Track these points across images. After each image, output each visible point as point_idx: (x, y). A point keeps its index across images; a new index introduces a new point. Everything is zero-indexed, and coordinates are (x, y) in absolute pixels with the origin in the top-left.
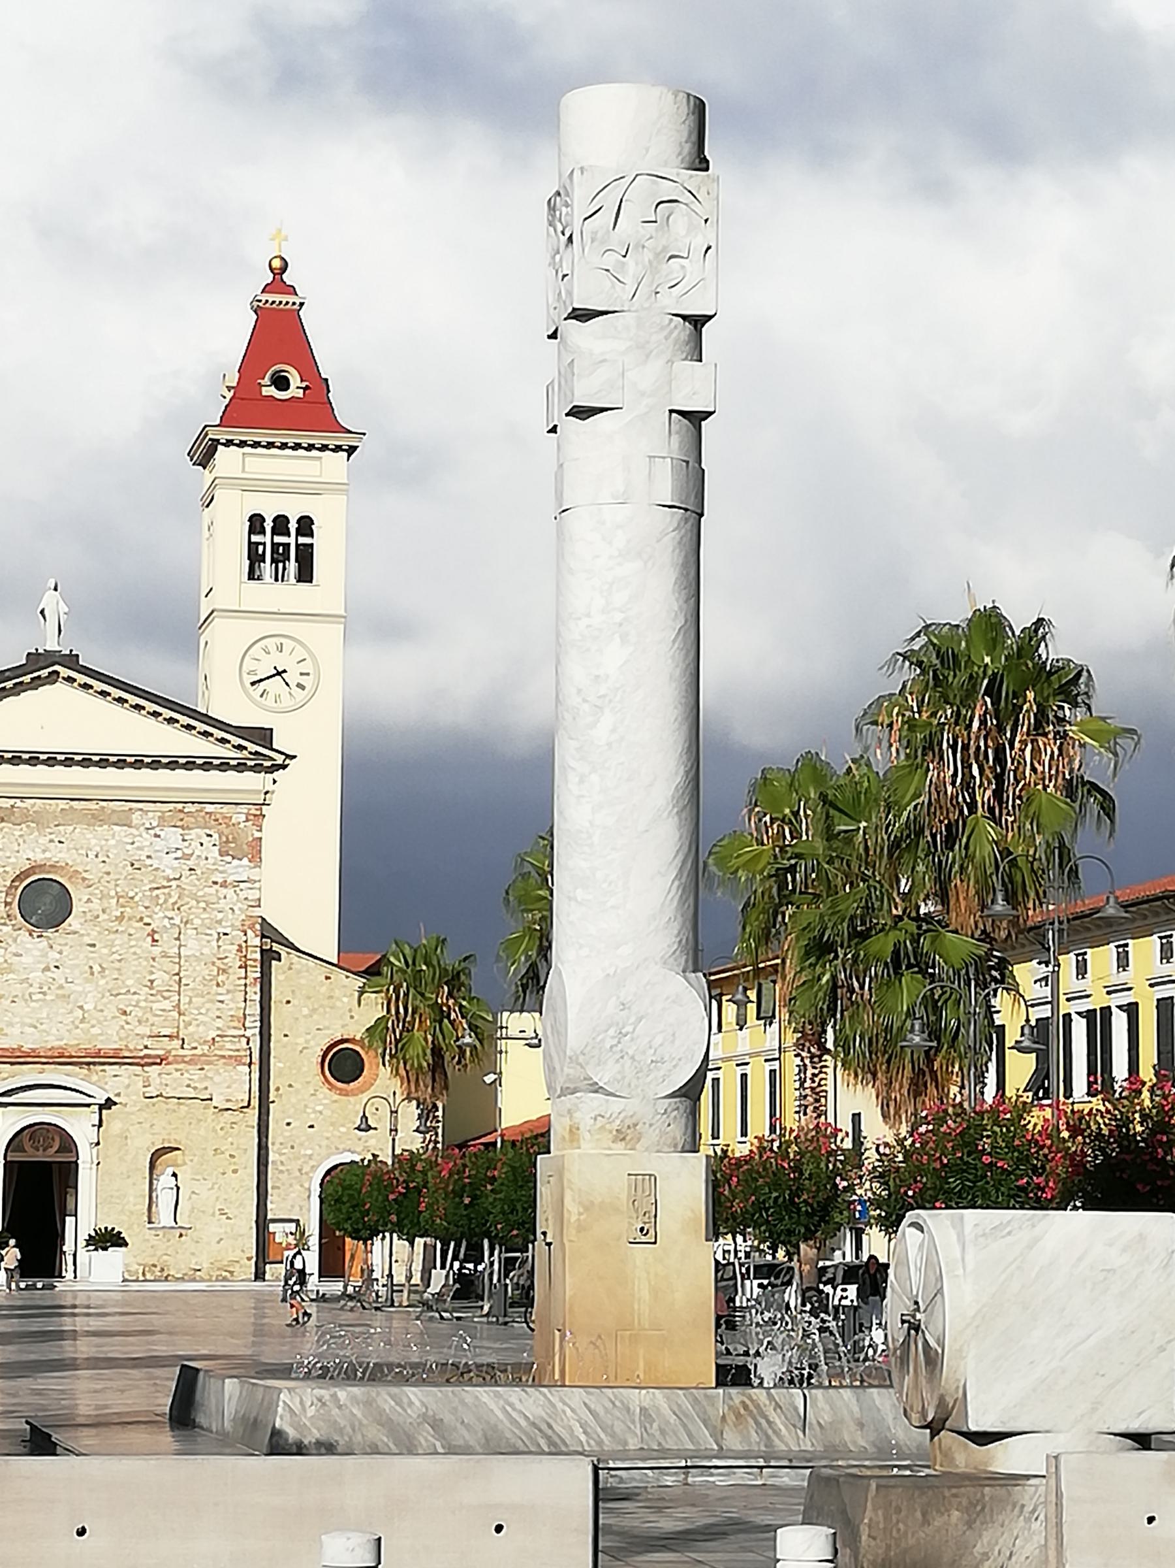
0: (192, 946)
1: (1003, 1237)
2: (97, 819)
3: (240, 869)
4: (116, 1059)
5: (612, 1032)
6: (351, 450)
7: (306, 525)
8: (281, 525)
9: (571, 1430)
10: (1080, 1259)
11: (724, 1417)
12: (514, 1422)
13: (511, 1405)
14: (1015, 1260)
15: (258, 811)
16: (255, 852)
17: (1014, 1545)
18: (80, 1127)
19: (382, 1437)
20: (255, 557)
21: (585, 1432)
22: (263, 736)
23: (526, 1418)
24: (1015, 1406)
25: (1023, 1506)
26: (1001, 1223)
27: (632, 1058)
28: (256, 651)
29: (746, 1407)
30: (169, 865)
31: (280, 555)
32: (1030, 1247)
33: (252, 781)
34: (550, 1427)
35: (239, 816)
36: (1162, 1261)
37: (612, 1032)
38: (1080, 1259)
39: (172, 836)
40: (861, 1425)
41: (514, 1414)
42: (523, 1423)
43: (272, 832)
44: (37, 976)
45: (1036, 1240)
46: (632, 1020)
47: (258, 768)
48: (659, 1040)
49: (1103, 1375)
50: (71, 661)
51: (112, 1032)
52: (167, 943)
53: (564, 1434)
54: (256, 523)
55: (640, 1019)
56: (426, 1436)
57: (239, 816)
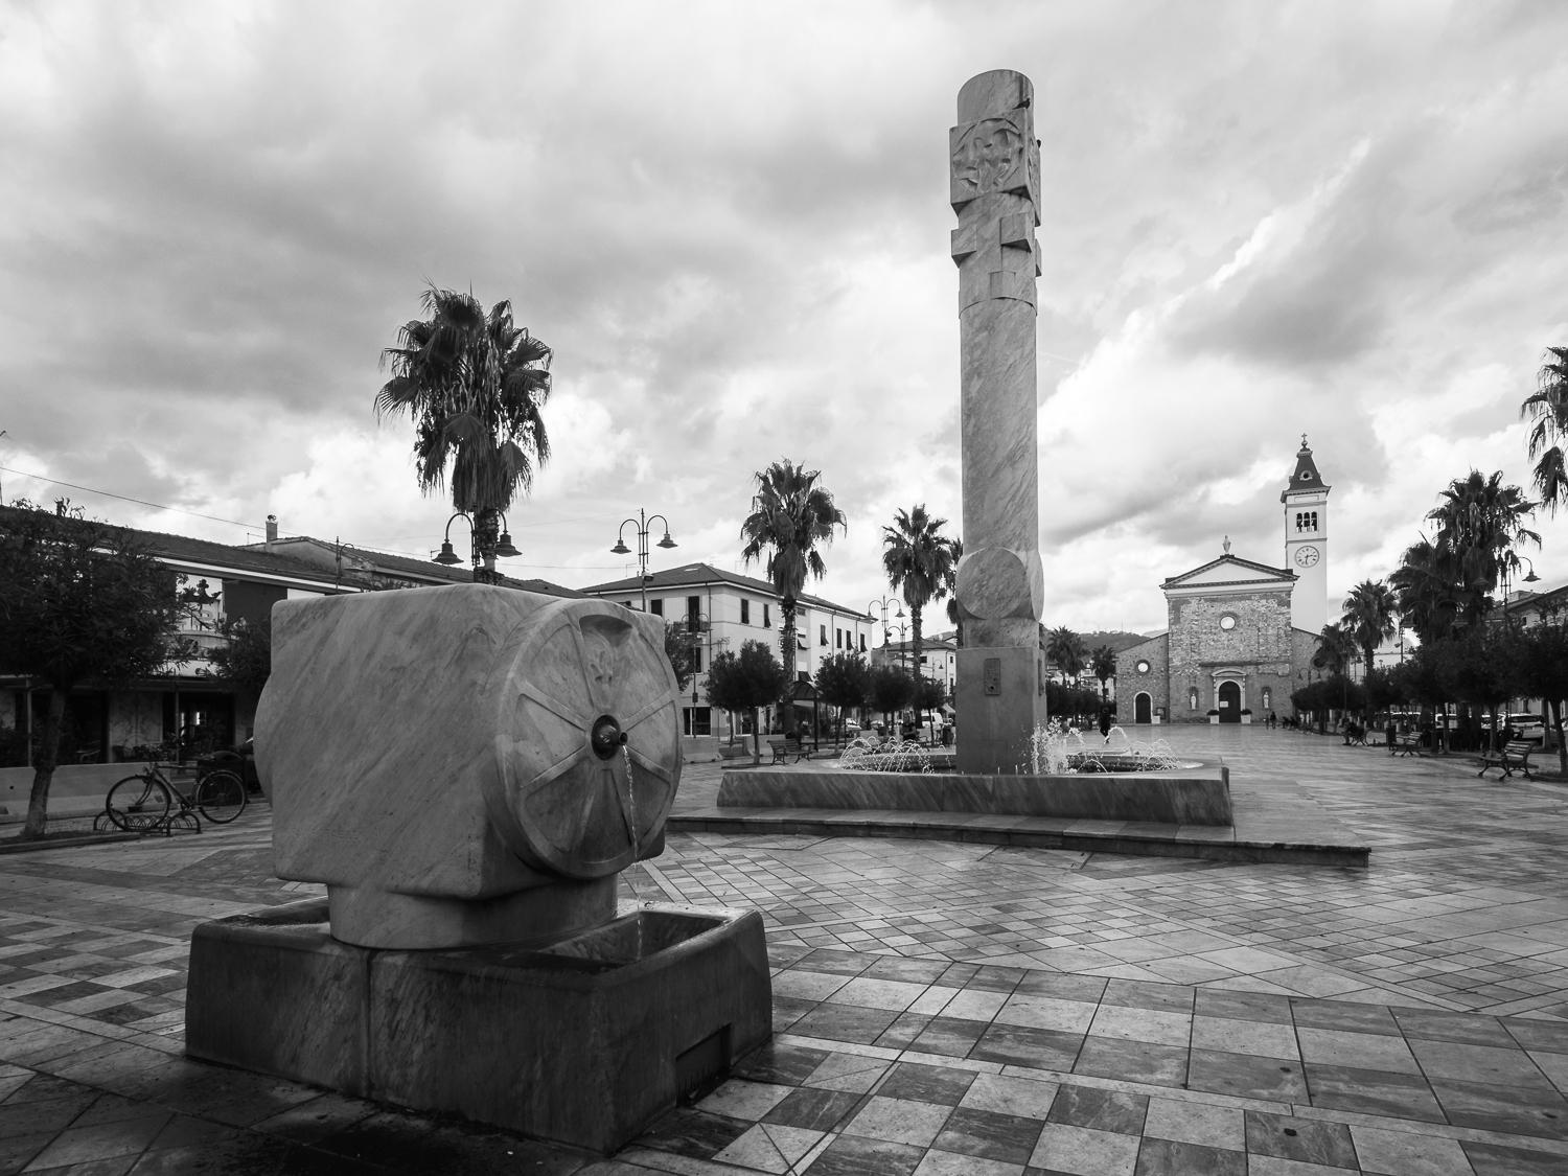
0: (1271, 632)
1: (298, 632)
2: (1241, 599)
3: (1284, 609)
4: (1250, 663)
5: (976, 585)
6: (1327, 492)
7: (1314, 515)
8: (1307, 515)
9: (860, 797)
10: (370, 656)
11: (943, 793)
12: (832, 792)
13: (832, 783)
14: (309, 660)
15: (1289, 594)
16: (1288, 604)
17: (306, 1028)
18: (1241, 684)
19: (767, 799)
20: (1299, 525)
21: (868, 799)
22: (1290, 571)
23: (838, 789)
24: (308, 851)
25: (313, 980)
26: (296, 615)
27: (987, 598)
28: (1301, 551)
29: (956, 787)
30: (1263, 609)
31: (1307, 524)
32: (323, 642)
33: (1290, 584)
34: (849, 795)
35: (1284, 595)
36: (456, 651)
37: (976, 585)
38: (370, 656)
39: (1264, 602)
40: (1028, 799)
41: (833, 788)
42: (836, 792)
43: (1293, 598)
44: (1226, 642)
45: (328, 633)
46: (987, 577)
47: (1289, 580)
48: (1001, 587)
49: (392, 814)
50: (1232, 557)
51: (1248, 656)
52: (1263, 631)
53: (856, 798)
54: (1299, 516)
55: (991, 577)
56: (787, 799)
57: (1284, 595)
